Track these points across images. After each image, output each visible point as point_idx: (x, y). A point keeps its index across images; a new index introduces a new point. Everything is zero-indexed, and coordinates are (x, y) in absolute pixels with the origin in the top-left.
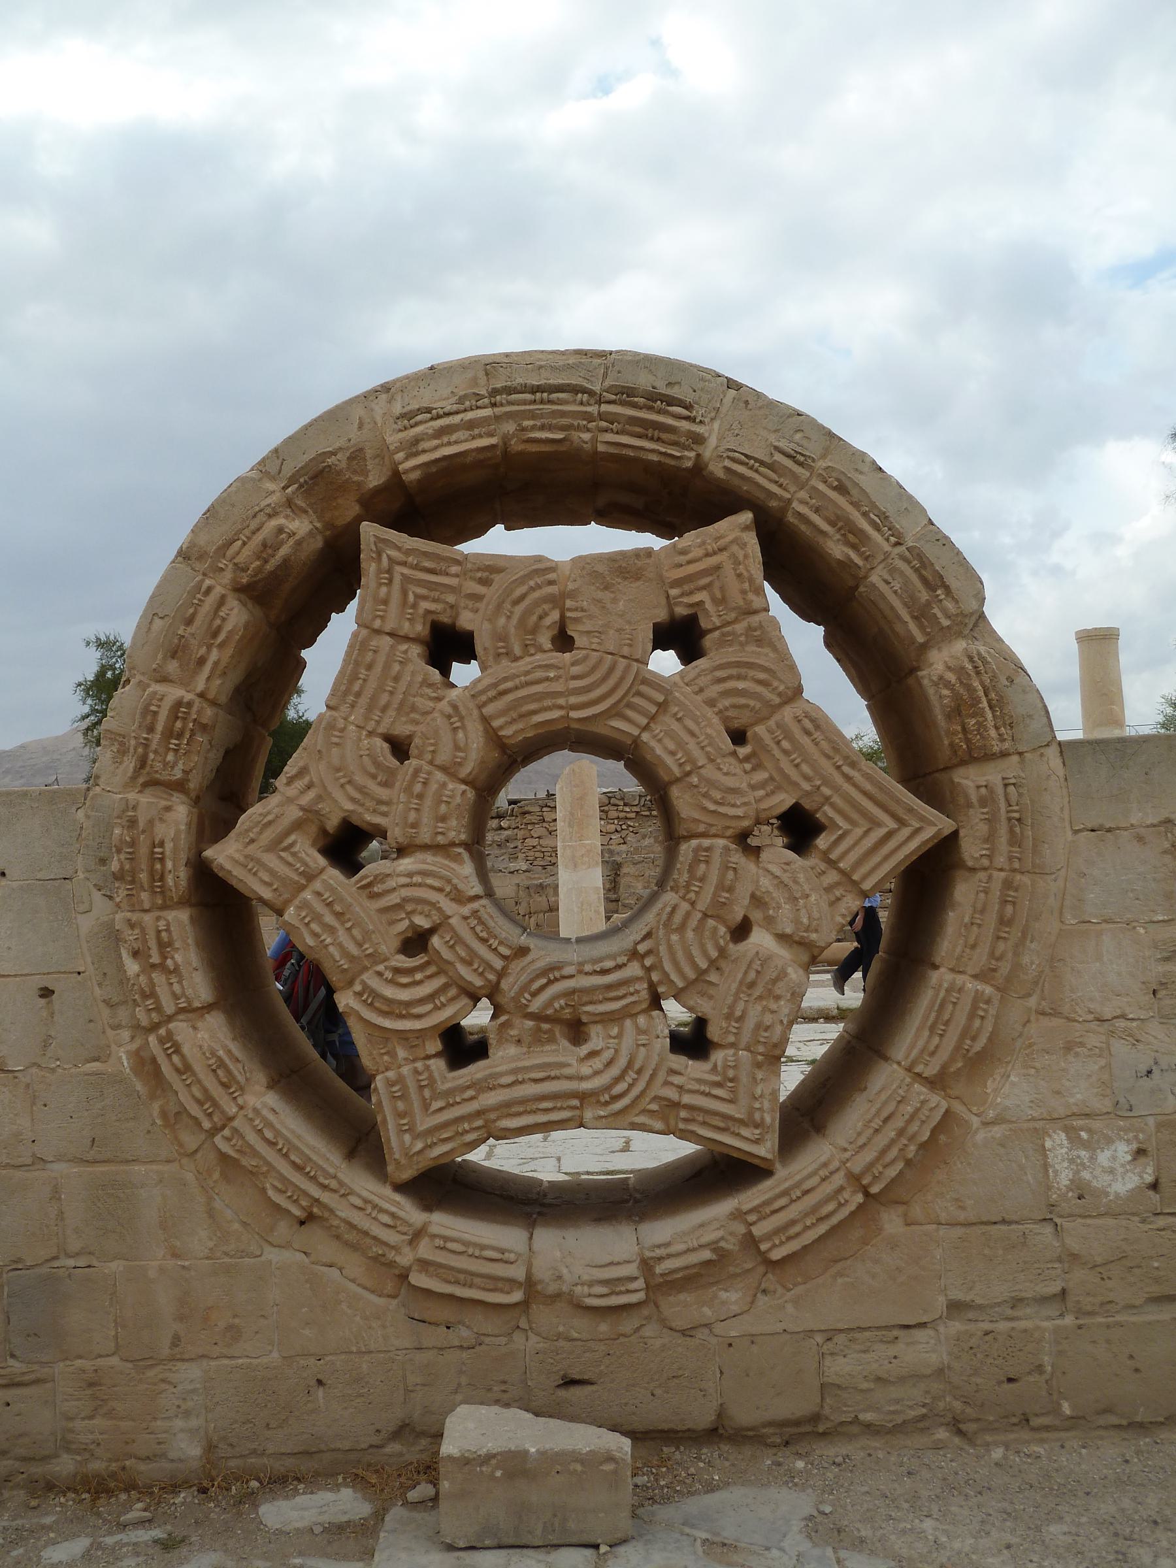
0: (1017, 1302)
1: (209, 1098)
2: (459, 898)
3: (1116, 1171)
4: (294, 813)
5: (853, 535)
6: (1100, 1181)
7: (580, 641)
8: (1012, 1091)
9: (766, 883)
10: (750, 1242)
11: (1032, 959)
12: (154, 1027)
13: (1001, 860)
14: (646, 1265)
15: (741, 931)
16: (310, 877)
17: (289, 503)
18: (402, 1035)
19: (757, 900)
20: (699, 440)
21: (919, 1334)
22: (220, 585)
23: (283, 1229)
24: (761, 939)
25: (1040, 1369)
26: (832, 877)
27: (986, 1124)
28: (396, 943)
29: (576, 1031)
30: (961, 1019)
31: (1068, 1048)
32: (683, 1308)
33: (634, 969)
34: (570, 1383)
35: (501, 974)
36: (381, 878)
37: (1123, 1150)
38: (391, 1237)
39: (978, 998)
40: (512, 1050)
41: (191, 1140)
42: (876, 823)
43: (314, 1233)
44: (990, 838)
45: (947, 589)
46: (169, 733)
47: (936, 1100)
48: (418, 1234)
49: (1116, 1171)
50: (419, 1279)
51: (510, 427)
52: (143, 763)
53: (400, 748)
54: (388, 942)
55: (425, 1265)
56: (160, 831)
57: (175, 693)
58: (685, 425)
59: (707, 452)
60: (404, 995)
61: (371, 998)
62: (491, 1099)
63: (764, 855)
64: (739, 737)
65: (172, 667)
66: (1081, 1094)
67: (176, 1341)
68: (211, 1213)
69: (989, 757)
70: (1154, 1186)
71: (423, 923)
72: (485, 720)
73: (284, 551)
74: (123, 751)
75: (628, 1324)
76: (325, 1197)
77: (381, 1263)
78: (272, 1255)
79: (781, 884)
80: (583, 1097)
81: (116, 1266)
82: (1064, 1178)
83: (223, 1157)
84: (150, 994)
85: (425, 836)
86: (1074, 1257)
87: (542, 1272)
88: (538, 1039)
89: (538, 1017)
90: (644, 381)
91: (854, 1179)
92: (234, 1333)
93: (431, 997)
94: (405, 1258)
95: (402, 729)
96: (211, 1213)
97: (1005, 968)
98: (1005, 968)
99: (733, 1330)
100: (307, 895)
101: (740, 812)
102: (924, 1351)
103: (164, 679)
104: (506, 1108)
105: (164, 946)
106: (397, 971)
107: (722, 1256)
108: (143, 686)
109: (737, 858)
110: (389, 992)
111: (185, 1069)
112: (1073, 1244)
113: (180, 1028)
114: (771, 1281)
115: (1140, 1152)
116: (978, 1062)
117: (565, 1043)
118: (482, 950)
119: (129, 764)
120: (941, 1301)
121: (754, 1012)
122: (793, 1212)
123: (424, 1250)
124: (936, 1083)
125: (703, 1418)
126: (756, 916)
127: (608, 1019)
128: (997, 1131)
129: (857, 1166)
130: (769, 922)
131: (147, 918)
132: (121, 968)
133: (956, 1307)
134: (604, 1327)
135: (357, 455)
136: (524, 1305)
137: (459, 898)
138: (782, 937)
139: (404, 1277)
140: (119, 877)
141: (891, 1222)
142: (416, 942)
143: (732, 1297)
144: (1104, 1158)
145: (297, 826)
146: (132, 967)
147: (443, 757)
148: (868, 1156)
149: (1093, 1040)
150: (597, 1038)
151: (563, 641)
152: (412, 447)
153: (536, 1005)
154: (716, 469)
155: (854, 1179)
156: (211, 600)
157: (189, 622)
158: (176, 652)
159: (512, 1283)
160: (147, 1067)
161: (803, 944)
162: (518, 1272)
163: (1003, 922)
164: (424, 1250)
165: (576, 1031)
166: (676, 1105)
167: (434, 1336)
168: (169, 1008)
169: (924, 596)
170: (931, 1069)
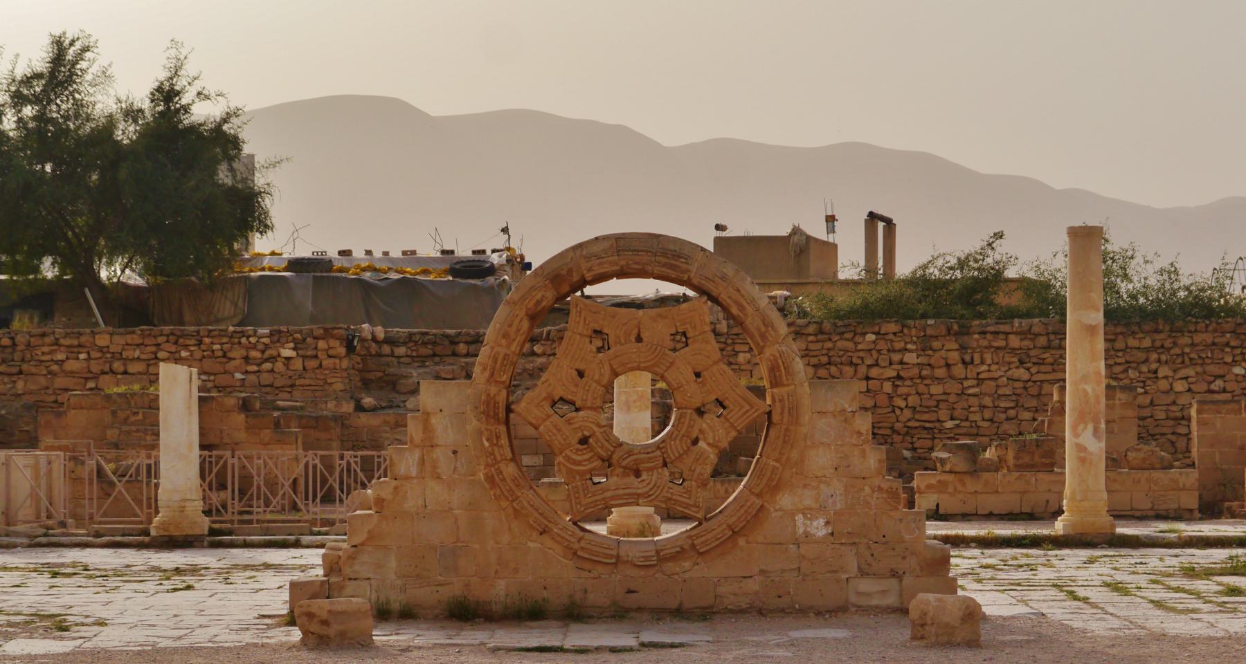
0: (783, 571)
1: (511, 490)
2: (599, 426)
3: (819, 528)
4: (544, 395)
5: (741, 308)
6: (813, 531)
7: (645, 339)
8: (785, 500)
9: (704, 425)
10: (693, 546)
11: (795, 455)
12: (493, 465)
13: (785, 420)
14: (658, 552)
15: (695, 442)
16: (549, 416)
17: (546, 286)
18: (578, 472)
19: (701, 431)
20: (688, 271)
21: (750, 581)
22: (522, 313)
23: (535, 535)
24: (702, 444)
25: (789, 593)
26: (727, 424)
27: (776, 511)
28: (576, 440)
29: (637, 474)
30: (768, 474)
31: (805, 486)
32: (669, 567)
33: (658, 453)
34: (630, 592)
35: (613, 453)
36: (573, 418)
37: (822, 521)
38: (573, 540)
39: (774, 468)
40: (615, 478)
41: (504, 504)
42: (742, 407)
43: (545, 538)
44: (782, 413)
45: (773, 328)
46: (502, 365)
47: (758, 502)
48: (580, 540)
49: (819, 528)
50: (579, 553)
51: (623, 263)
52: (492, 374)
53: (581, 374)
54: (574, 440)
55: (582, 548)
56: (497, 398)
57: (503, 351)
58: (684, 266)
59: (692, 275)
60: (579, 458)
61: (568, 458)
62: (609, 494)
63: (706, 416)
64: (698, 375)
65: (504, 342)
66: (808, 502)
67: (496, 572)
68: (510, 529)
69: (784, 385)
70: (832, 534)
71: (587, 433)
72: (611, 366)
73: (544, 303)
74: (484, 369)
75: (651, 571)
76: (550, 525)
77: (567, 547)
78: (530, 544)
79: (710, 427)
80: (639, 495)
81: (477, 546)
82: (801, 531)
83: (515, 510)
84: (493, 454)
85: (589, 404)
86: (803, 557)
87: (622, 553)
88: (624, 475)
89: (625, 468)
90: (671, 247)
91: (730, 527)
92: (516, 570)
93: (588, 460)
94: (576, 546)
95: (582, 367)
96: (510, 529)
97: (785, 458)
98: (785, 458)
99: (687, 576)
100: (548, 423)
101: (697, 402)
102: (753, 585)
103: (500, 345)
104: (612, 498)
105: (498, 437)
106: (578, 450)
107: (683, 551)
108: (493, 348)
109: (695, 416)
110: (574, 457)
111: (504, 480)
112: (802, 551)
113: (502, 466)
114: (699, 560)
115: (827, 523)
116: (775, 487)
117: (633, 478)
118: (606, 444)
119: (487, 374)
120: (756, 570)
121: (698, 470)
122: (709, 536)
123: (583, 544)
124: (759, 495)
125: (674, 605)
126: (701, 436)
127: (651, 469)
128: (779, 513)
129: (731, 521)
130: (705, 439)
131: (492, 428)
132: (483, 445)
133: (762, 572)
134: (642, 573)
135: (570, 271)
136: (615, 564)
137: (599, 426)
138: (709, 444)
139: (575, 553)
140: (483, 413)
141: (742, 542)
142: (584, 441)
143: (687, 564)
144: (815, 523)
145: (545, 399)
146: (487, 444)
147: (596, 377)
148: (734, 519)
149: (814, 484)
150: (644, 476)
151: (639, 339)
152: (589, 270)
153: (624, 464)
154: (695, 281)
155: (730, 527)
156: (518, 319)
157: (510, 326)
158: (506, 335)
159: (612, 556)
160: (490, 479)
161: (717, 447)
162: (614, 553)
163: (784, 442)
164: (583, 544)
165: (637, 474)
166: (670, 499)
167: (586, 574)
168: (499, 458)
169: (763, 329)
170: (757, 491)
